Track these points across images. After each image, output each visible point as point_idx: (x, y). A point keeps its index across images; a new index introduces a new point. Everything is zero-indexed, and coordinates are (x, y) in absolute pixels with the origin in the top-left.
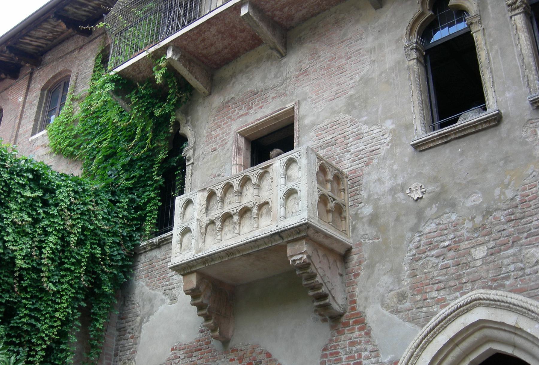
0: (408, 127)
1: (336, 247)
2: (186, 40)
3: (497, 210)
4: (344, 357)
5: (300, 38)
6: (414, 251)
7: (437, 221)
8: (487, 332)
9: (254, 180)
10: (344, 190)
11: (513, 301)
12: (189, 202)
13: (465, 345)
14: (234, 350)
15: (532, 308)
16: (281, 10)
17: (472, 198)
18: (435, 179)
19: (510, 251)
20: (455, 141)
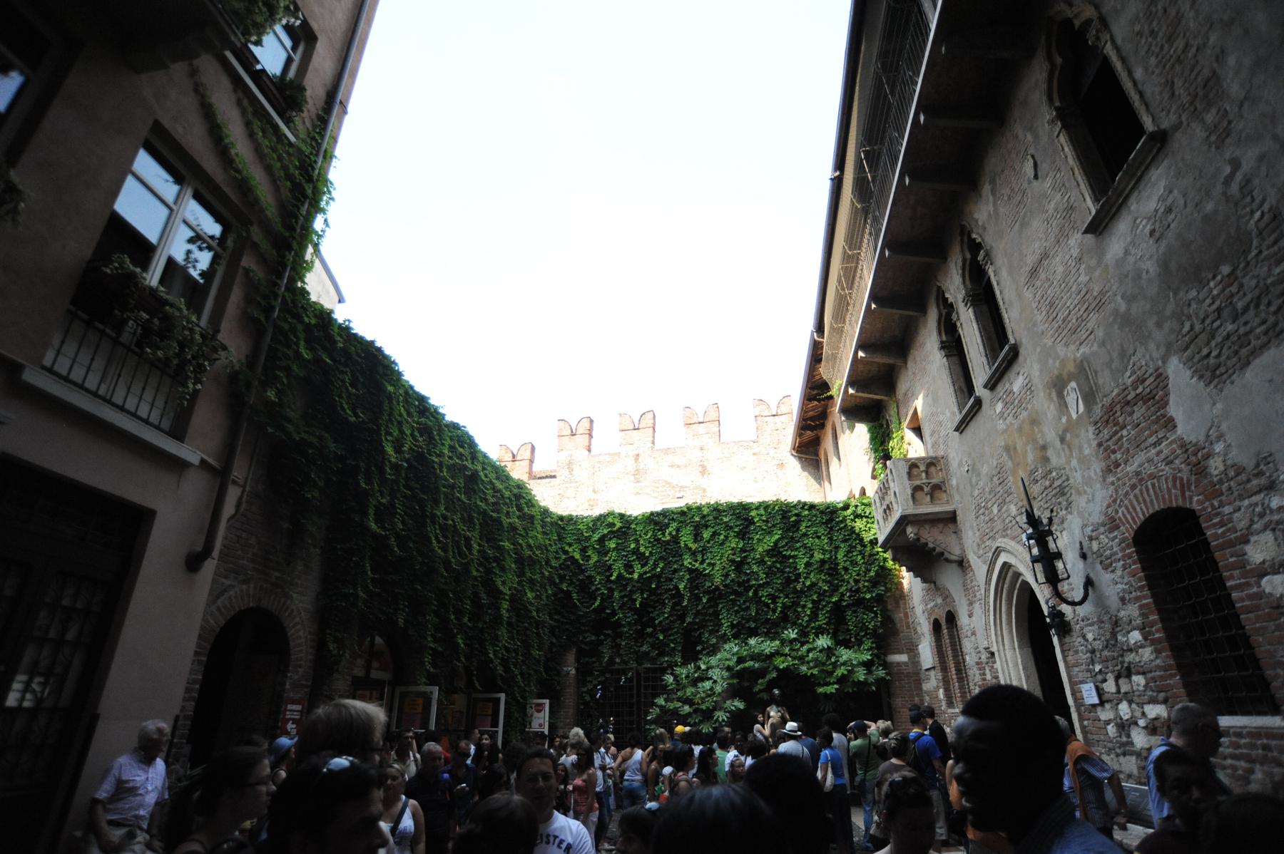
1: (940, 516)
10: (941, 470)
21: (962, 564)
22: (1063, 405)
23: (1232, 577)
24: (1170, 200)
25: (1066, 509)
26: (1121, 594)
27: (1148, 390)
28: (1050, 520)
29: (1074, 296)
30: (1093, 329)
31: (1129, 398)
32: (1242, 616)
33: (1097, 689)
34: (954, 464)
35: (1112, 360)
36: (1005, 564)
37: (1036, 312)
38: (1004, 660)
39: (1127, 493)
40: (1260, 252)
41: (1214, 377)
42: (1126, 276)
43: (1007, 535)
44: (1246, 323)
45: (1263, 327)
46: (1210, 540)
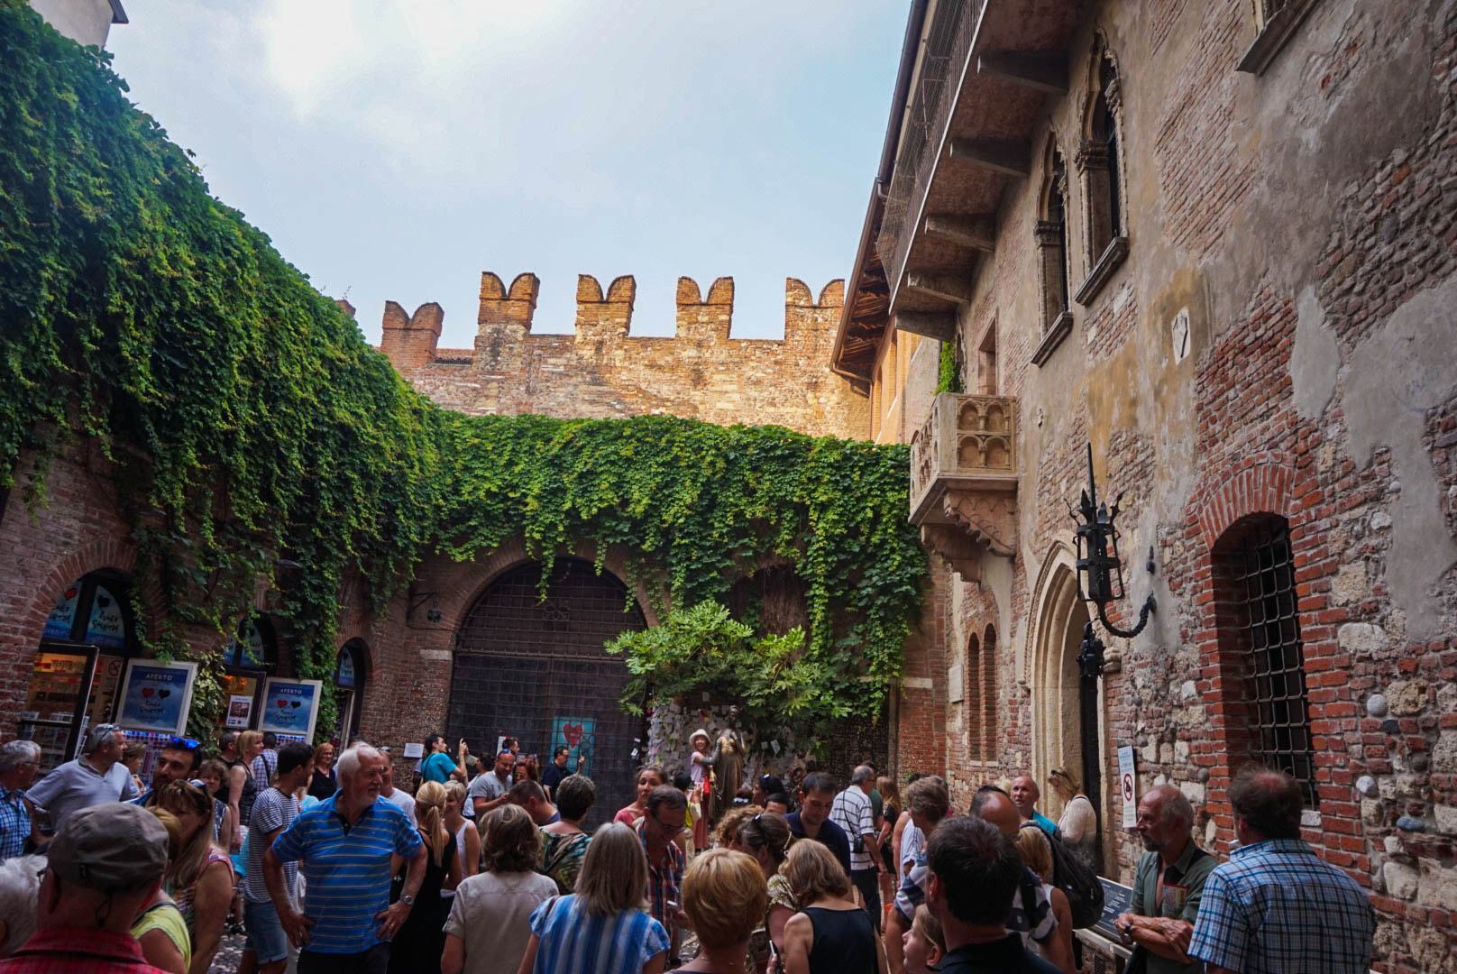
1: (995, 487)
10: (1008, 418)
21: (1014, 559)
22: (1168, 341)
23: (1308, 621)
24: (1358, 29)
25: (1144, 498)
27: (1270, 333)
28: (1115, 510)
29: (1212, 172)
31: (1247, 341)
32: (1308, 676)
33: (1135, 752)
34: (1026, 413)
35: (1236, 281)
36: (1062, 566)
37: (1161, 191)
39: (1217, 484)
40: (1446, 133)
41: (1350, 324)
42: (1281, 149)
44: (1404, 246)
45: (1422, 255)
46: (1296, 565)
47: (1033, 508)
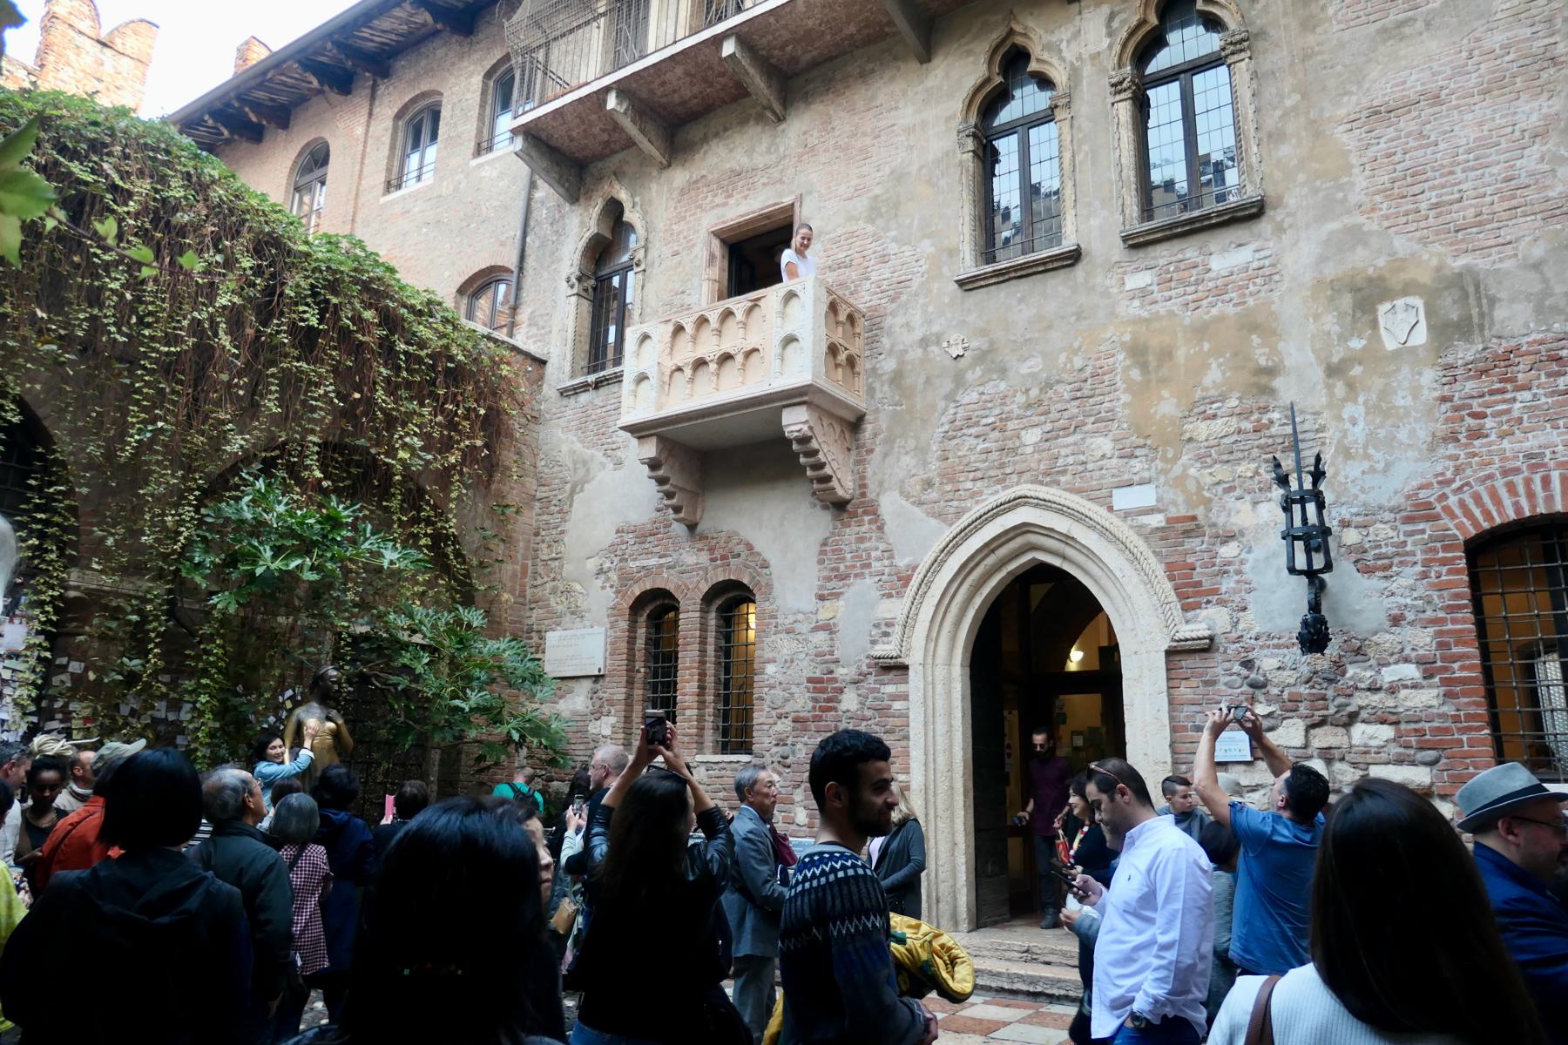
0: (952, 253)
2: (637, 81)
3: (1058, 382)
4: (848, 556)
5: (807, 93)
6: (946, 427)
7: (981, 389)
8: (1033, 538)
9: (740, 315)
11: (1067, 503)
12: (645, 337)
13: (1002, 552)
14: (703, 537)
15: (1090, 514)
16: (782, 48)
17: (1029, 363)
18: (983, 332)
19: (1071, 439)
20: (1013, 282)
26: (1396, 612)
30: (1517, 240)
38: (930, 679)
39: (1490, 477)
43: (1058, 483)
47: (921, 451)
